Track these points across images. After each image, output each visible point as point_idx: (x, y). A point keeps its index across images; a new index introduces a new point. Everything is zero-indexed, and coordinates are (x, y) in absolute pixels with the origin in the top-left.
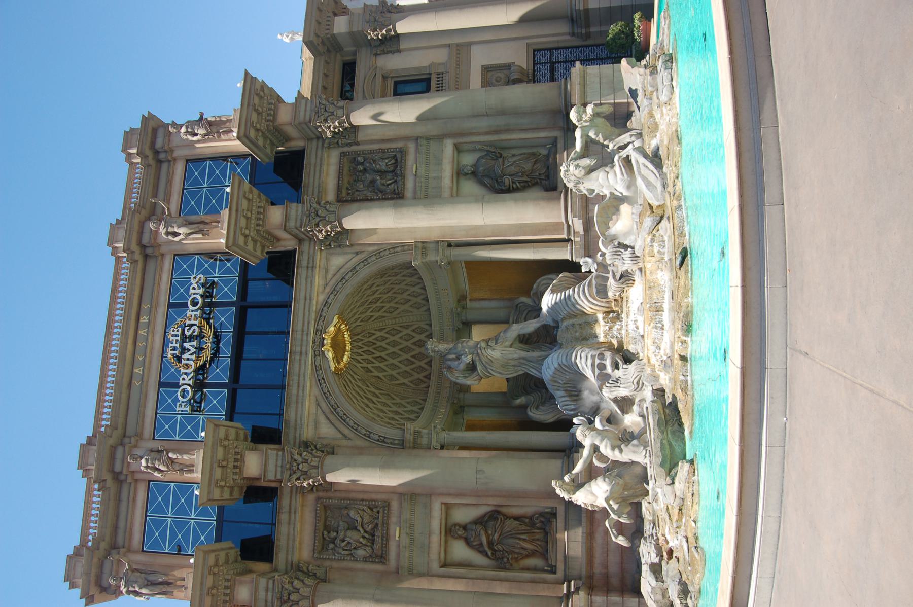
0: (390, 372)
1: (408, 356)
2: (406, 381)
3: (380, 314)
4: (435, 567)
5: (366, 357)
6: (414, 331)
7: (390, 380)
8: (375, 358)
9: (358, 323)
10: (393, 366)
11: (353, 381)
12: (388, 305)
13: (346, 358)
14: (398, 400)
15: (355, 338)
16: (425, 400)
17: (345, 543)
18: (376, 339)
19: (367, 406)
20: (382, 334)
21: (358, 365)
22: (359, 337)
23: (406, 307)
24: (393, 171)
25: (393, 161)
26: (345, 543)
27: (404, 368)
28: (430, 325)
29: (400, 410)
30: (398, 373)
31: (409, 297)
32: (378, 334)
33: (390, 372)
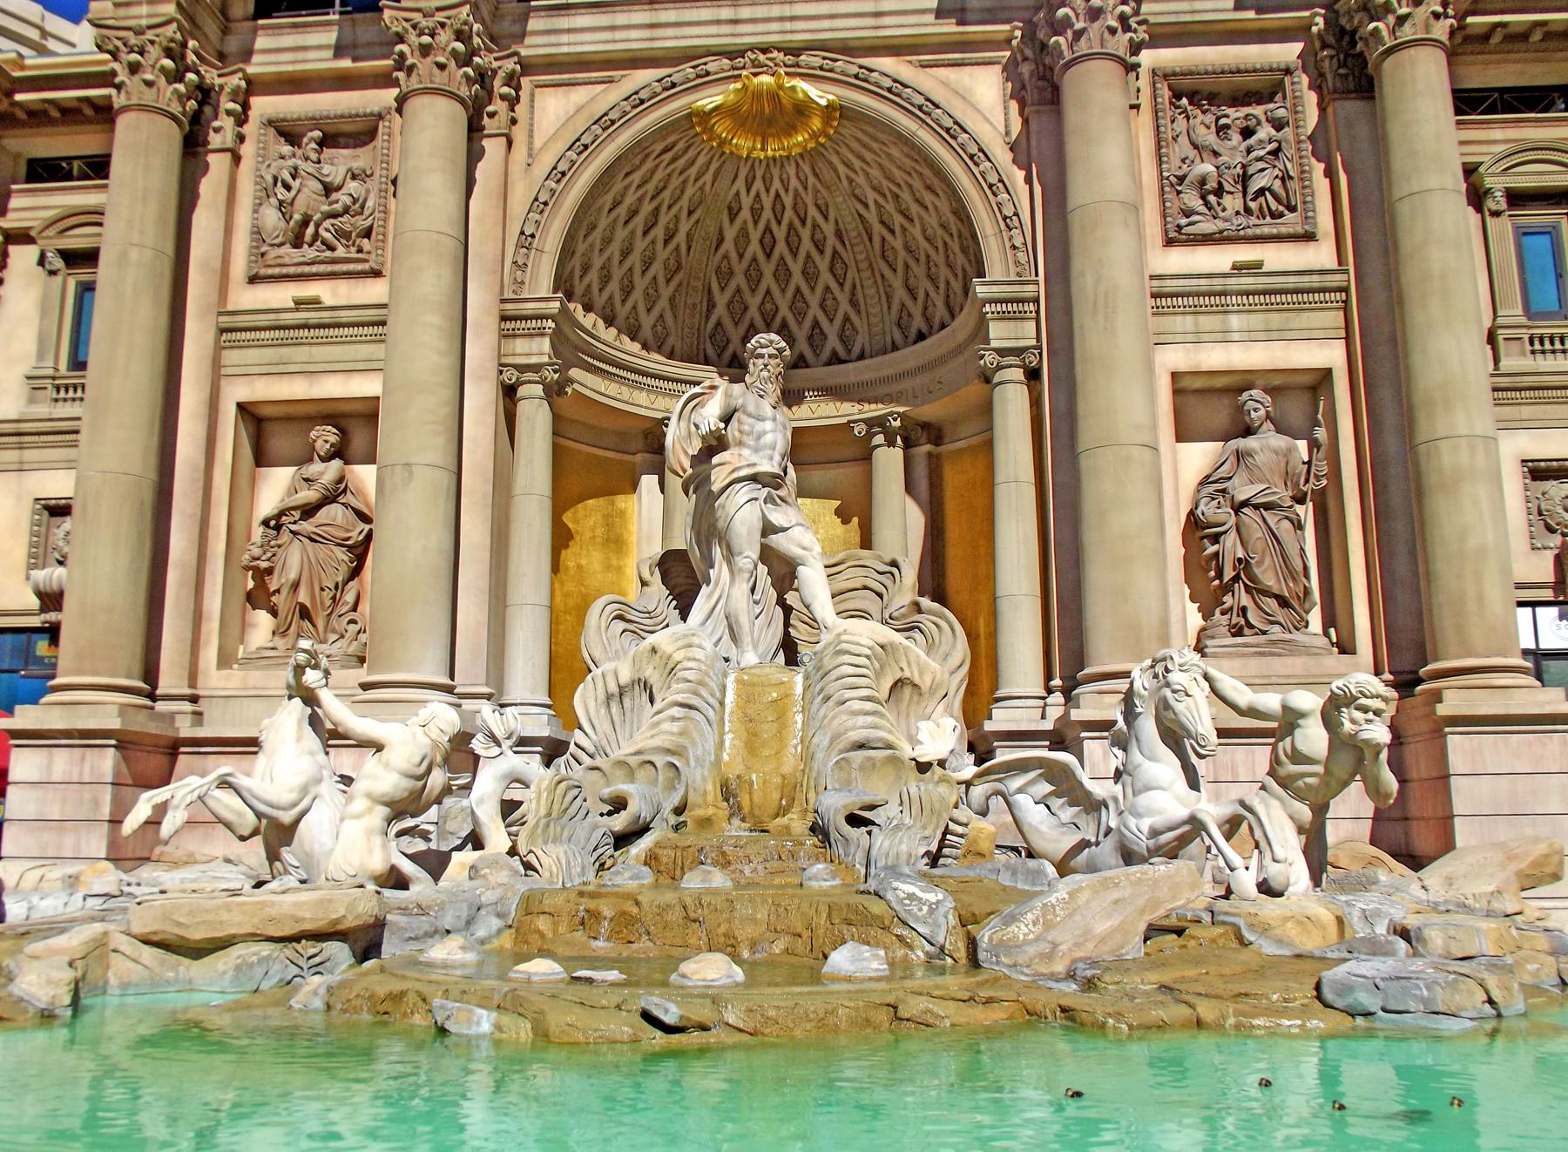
0: (739, 268)
1: (784, 311)
2: (720, 311)
3: (877, 228)
4: (237, 392)
5: (767, 201)
6: (847, 319)
7: (718, 271)
8: (768, 229)
9: (842, 169)
10: (754, 278)
11: (693, 171)
12: (898, 243)
13: (743, 144)
14: (666, 293)
15: (806, 168)
16: (671, 356)
17: (289, 179)
18: (815, 226)
19: (633, 213)
20: (831, 241)
21: (740, 184)
22: (811, 180)
23: (900, 293)
24: (1248, 211)
25: (1274, 205)
26: (289, 179)
27: (754, 302)
28: (861, 357)
29: (638, 295)
30: (738, 291)
31: (921, 297)
32: (828, 229)
33: (739, 268)
